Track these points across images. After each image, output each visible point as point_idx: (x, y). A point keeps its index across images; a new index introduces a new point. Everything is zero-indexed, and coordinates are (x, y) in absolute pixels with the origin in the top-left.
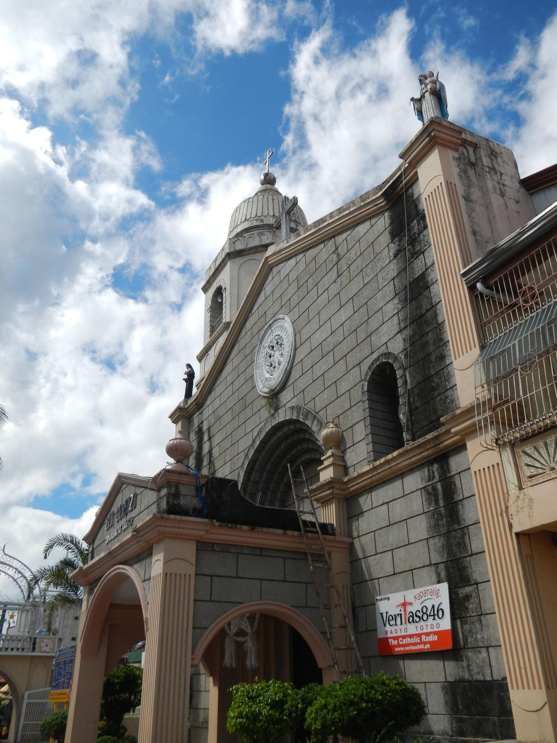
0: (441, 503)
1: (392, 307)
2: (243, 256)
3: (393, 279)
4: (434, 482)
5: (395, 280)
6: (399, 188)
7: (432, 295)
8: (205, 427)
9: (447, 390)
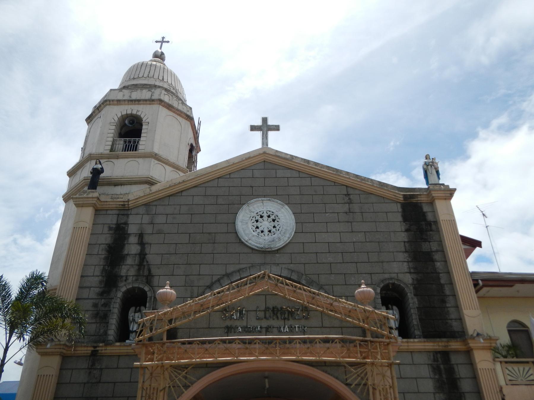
0: (444, 376)
1: (402, 257)
2: (170, 110)
3: (404, 242)
4: (438, 363)
5: (406, 243)
6: (414, 199)
7: (436, 267)
8: (132, 229)
9: (448, 319)
